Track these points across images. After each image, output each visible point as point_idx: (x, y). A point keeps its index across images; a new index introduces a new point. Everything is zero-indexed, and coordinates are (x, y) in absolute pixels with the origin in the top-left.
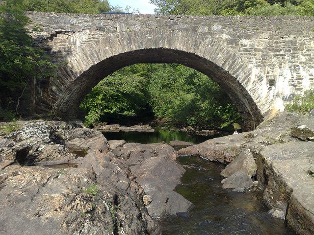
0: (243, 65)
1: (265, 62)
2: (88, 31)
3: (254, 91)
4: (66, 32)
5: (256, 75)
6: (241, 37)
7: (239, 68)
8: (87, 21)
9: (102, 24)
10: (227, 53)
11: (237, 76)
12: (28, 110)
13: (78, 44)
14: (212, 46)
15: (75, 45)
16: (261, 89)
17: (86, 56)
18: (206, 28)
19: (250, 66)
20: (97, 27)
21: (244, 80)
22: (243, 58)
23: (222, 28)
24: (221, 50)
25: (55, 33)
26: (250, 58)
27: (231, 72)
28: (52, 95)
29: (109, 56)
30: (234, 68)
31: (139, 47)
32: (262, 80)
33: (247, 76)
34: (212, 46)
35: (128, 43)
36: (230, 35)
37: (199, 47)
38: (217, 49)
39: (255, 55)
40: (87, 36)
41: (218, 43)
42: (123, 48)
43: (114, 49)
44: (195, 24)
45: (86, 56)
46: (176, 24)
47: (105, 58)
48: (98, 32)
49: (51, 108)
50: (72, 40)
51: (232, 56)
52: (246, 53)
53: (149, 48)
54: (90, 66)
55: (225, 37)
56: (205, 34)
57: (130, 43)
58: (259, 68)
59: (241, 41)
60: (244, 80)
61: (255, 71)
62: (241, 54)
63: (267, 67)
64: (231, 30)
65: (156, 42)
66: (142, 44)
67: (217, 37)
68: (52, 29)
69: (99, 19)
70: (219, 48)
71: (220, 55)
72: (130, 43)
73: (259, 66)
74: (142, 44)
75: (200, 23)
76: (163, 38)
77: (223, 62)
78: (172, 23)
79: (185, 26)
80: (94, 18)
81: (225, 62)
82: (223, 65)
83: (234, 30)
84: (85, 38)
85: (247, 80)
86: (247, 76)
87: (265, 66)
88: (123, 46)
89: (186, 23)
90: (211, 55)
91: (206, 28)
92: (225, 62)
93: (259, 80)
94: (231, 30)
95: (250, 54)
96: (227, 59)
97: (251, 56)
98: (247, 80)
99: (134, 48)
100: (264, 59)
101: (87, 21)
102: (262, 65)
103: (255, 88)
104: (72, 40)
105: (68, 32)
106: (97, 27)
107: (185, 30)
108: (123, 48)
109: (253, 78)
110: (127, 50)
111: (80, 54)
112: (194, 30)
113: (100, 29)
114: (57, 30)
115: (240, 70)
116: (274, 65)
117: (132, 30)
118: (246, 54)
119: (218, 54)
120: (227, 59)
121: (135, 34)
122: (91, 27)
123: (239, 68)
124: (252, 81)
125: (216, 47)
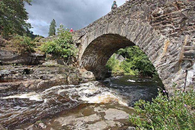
7: (149, 42)
32: (176, 55)
70: (133, 25)
73: (174, 36)
77: (135, 37)
123: (149, 42)
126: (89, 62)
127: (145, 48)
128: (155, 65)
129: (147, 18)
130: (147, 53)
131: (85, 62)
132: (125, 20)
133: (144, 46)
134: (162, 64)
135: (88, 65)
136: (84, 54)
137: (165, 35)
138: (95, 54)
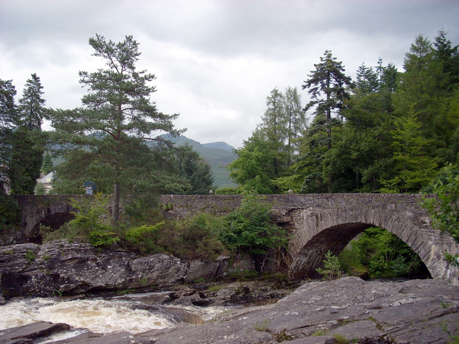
0: (423, 242)
1: (443, 240)
2: (311, 208)
3: (433, 268)
4: (298, 209)
5: (435, 253)
6: (421, 214)
7: (420, 245)
8: (310, 200)
9: (320, 202)
10: (411, 230)
11: (419, 252)
12: (271, 270)
13: (305, 218)
14: (399, 222)
15: (303, 219)
16: (440, 267)
17: (310, 228)
18: (393, 205)
19: (430, 242)
20: (317, 205)
21: (424, 257)
22: (424, 236)
23: (406, 205)
24: (405, 227)
25: (291, 210)
26: (430, 236)
27: (414, 248)
28: (289, 258)
29: (324, 229)
30: (416, 244)
31: (344, 221)
33: (427, 253)
34: (399, 222)
35: (336, 218)
36: (412, 213)
37: (388, 223)
38: (402, 225)
39: (434, 232)
40: (311, 212)
41: (403, 220)
42: (333, 222)
43: (327, 223)
44: (384, 201)
45: (310, 228)
46: (370, 201)
47: (322, 230)
48: (318, 209)
49: (287, 268)
50: (301, 215)
51: (415, 232)
52: (426, 230)
53: (351, 222)
54: (312, 236)
55: (409, 214)
56: (392, 211)
57: (338, 218)
58: (438, 246)
59: (422, 218)
60: (424, 257)
61: (434, 249)
62: (422, 231)
63: (445, 245)
64: (413, 208)
65: (356, 218)
66: (346, 219)
67: (402, 214)
68: (289, 207)
69: (318, 198)
70: (404, 224)
71: (405, 232)
72: (338, 218)
73: (438, 243)
74: (346, 219)
75: (388, 201)
76: (361, 214)
77: (407, 238)
78: (367, 201)
79: (377, 204)
80: (315, 197)
81: (409, 238)
82: (407, 241)
83: (416, 208)
84: (309, 213)
85: (427, 257)
86: (427, 253)
87: (443, 244)
88: (333, 219)
89: (378, 201)
90: (397, 231)
91: (393, 205)
92: (409, 238)
93: (437, 258)
94: (413, 208)
95: (429, 231)
96: (411, 235)
97: (431, 234)
98: (427, 257)
99: (341, 222)
100: (442, 237)
101: (310, 200)
102: (440, 243)
103: (434, 265)
104: (301, 215)
105: (299, 208)
106: (317, 205)
107: (377, 206)
108: (333, 222)
109: (432, 255)
110: (336, 224)
111: (306, 226)
112: (384, 207)
113: (318, 206)
114: (292, 208)
115: (421, 247)
116: (451, 243)
117: (339, 207)
118: (427, 232)
119: (403, 230)
120: (411, 235)
121: (341, 210)
122: (313, 204)
123: (420, 245)
124: (431, 258)
125: (401, 223)
126: (308, 260)
127: (418, 250)
128: (427, 266)
129: (416, 221)
130: (420, 255)
131: (301, 262)
132: (394, 215)
133: (417, 248)
134: (433, 265)
135: (305, 266)
136: (305, 247)
137: (432, 241)
138: (323, 243)
